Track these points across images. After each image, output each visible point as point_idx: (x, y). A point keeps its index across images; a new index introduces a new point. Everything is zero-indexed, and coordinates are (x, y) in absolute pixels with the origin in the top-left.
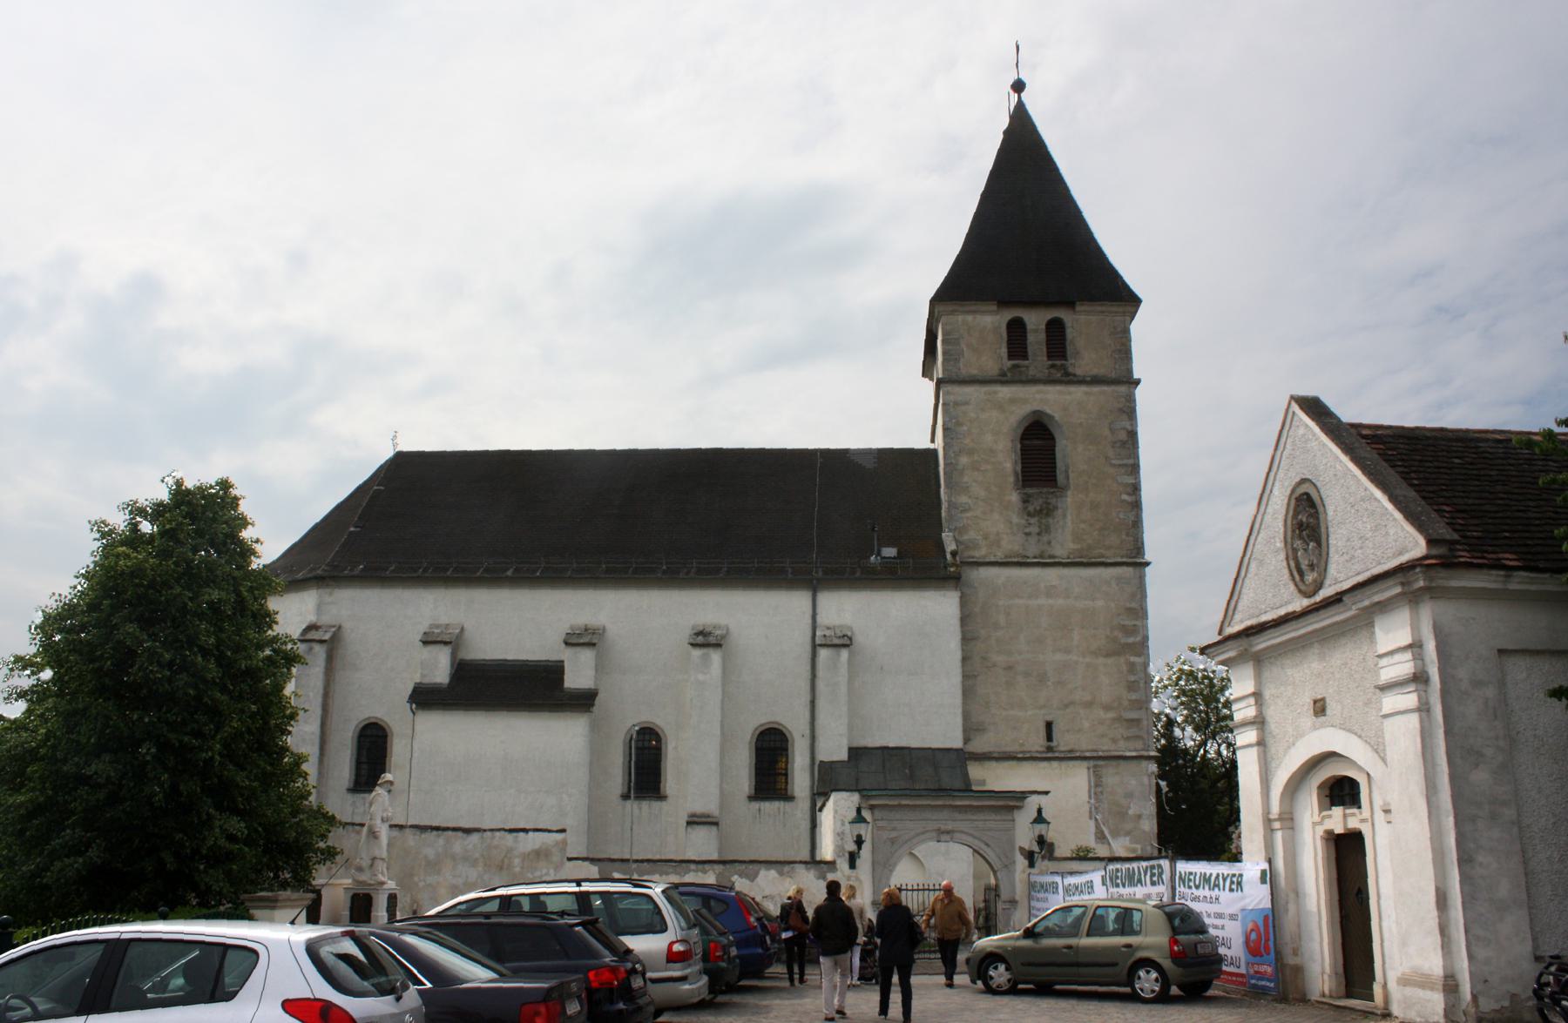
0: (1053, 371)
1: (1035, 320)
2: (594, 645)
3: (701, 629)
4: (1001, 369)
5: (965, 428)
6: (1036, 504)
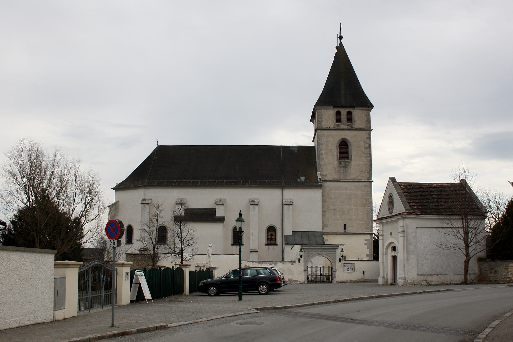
1: (344, 112)
6: (343, 164)
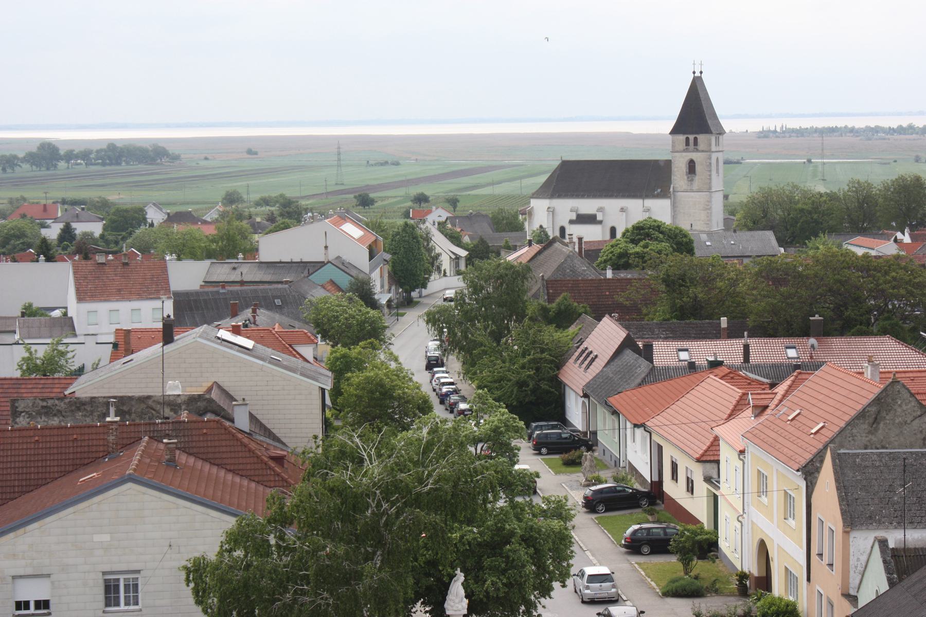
1: (691, 137)
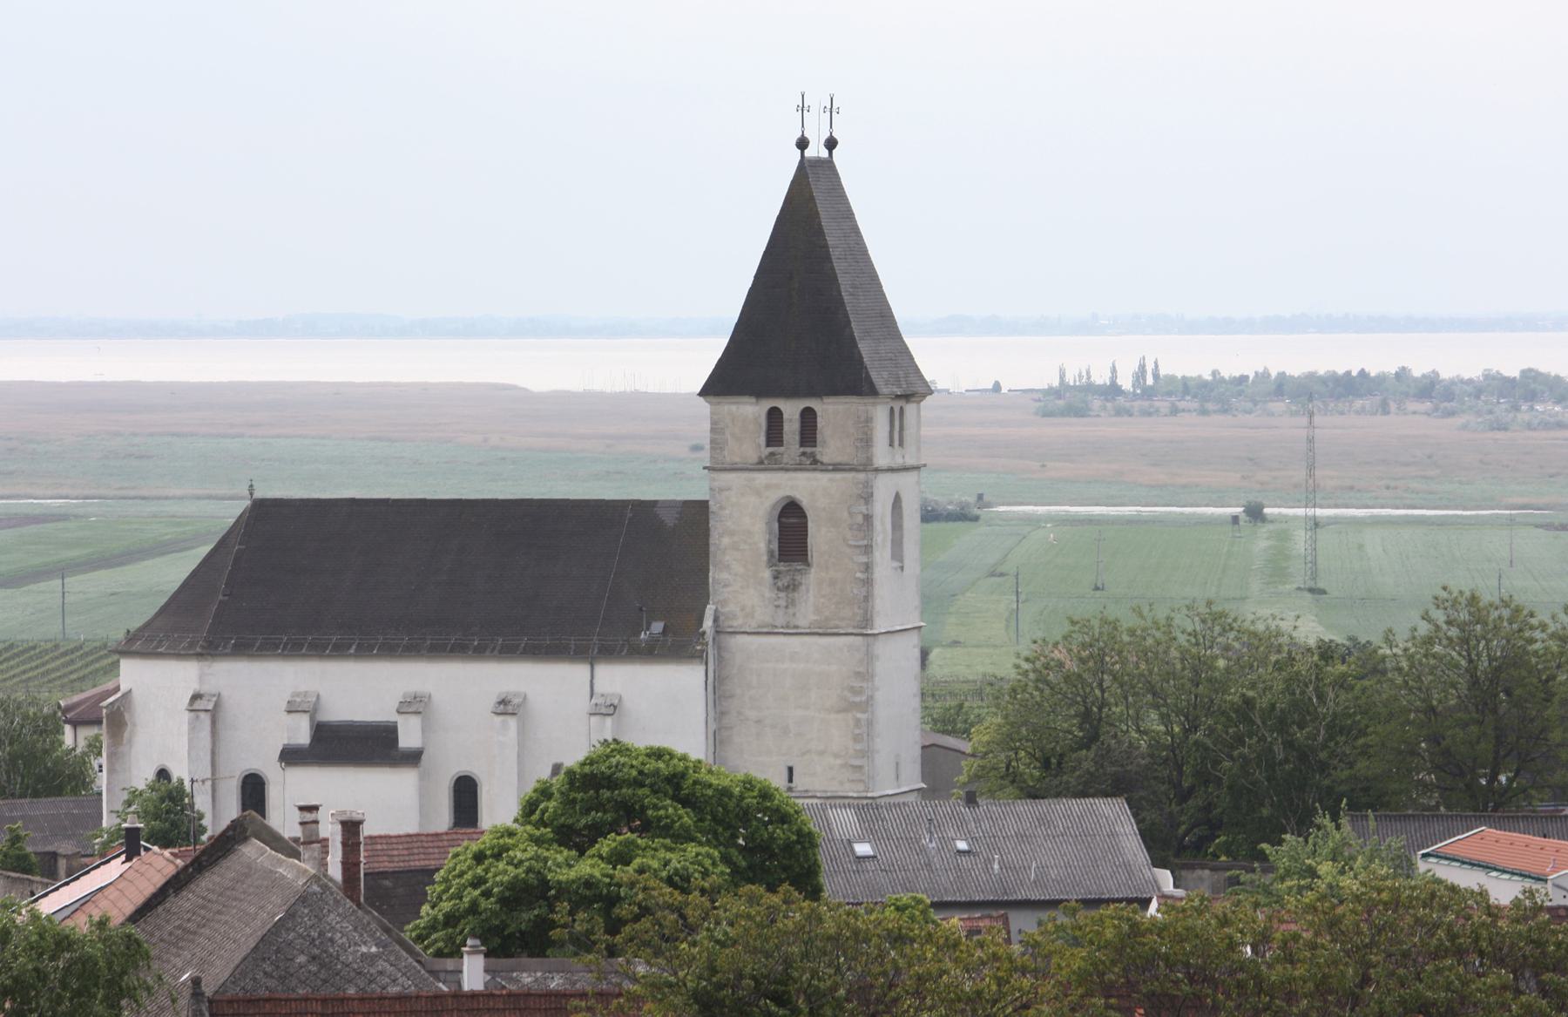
0: (803, 458)
1: (791, 410)
2: (420, 713)
3: (503, 697)
4: (760, 457)
5: (727, 512)
6: (784, 581)
